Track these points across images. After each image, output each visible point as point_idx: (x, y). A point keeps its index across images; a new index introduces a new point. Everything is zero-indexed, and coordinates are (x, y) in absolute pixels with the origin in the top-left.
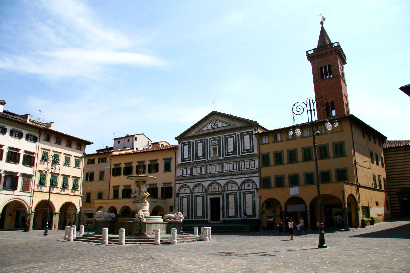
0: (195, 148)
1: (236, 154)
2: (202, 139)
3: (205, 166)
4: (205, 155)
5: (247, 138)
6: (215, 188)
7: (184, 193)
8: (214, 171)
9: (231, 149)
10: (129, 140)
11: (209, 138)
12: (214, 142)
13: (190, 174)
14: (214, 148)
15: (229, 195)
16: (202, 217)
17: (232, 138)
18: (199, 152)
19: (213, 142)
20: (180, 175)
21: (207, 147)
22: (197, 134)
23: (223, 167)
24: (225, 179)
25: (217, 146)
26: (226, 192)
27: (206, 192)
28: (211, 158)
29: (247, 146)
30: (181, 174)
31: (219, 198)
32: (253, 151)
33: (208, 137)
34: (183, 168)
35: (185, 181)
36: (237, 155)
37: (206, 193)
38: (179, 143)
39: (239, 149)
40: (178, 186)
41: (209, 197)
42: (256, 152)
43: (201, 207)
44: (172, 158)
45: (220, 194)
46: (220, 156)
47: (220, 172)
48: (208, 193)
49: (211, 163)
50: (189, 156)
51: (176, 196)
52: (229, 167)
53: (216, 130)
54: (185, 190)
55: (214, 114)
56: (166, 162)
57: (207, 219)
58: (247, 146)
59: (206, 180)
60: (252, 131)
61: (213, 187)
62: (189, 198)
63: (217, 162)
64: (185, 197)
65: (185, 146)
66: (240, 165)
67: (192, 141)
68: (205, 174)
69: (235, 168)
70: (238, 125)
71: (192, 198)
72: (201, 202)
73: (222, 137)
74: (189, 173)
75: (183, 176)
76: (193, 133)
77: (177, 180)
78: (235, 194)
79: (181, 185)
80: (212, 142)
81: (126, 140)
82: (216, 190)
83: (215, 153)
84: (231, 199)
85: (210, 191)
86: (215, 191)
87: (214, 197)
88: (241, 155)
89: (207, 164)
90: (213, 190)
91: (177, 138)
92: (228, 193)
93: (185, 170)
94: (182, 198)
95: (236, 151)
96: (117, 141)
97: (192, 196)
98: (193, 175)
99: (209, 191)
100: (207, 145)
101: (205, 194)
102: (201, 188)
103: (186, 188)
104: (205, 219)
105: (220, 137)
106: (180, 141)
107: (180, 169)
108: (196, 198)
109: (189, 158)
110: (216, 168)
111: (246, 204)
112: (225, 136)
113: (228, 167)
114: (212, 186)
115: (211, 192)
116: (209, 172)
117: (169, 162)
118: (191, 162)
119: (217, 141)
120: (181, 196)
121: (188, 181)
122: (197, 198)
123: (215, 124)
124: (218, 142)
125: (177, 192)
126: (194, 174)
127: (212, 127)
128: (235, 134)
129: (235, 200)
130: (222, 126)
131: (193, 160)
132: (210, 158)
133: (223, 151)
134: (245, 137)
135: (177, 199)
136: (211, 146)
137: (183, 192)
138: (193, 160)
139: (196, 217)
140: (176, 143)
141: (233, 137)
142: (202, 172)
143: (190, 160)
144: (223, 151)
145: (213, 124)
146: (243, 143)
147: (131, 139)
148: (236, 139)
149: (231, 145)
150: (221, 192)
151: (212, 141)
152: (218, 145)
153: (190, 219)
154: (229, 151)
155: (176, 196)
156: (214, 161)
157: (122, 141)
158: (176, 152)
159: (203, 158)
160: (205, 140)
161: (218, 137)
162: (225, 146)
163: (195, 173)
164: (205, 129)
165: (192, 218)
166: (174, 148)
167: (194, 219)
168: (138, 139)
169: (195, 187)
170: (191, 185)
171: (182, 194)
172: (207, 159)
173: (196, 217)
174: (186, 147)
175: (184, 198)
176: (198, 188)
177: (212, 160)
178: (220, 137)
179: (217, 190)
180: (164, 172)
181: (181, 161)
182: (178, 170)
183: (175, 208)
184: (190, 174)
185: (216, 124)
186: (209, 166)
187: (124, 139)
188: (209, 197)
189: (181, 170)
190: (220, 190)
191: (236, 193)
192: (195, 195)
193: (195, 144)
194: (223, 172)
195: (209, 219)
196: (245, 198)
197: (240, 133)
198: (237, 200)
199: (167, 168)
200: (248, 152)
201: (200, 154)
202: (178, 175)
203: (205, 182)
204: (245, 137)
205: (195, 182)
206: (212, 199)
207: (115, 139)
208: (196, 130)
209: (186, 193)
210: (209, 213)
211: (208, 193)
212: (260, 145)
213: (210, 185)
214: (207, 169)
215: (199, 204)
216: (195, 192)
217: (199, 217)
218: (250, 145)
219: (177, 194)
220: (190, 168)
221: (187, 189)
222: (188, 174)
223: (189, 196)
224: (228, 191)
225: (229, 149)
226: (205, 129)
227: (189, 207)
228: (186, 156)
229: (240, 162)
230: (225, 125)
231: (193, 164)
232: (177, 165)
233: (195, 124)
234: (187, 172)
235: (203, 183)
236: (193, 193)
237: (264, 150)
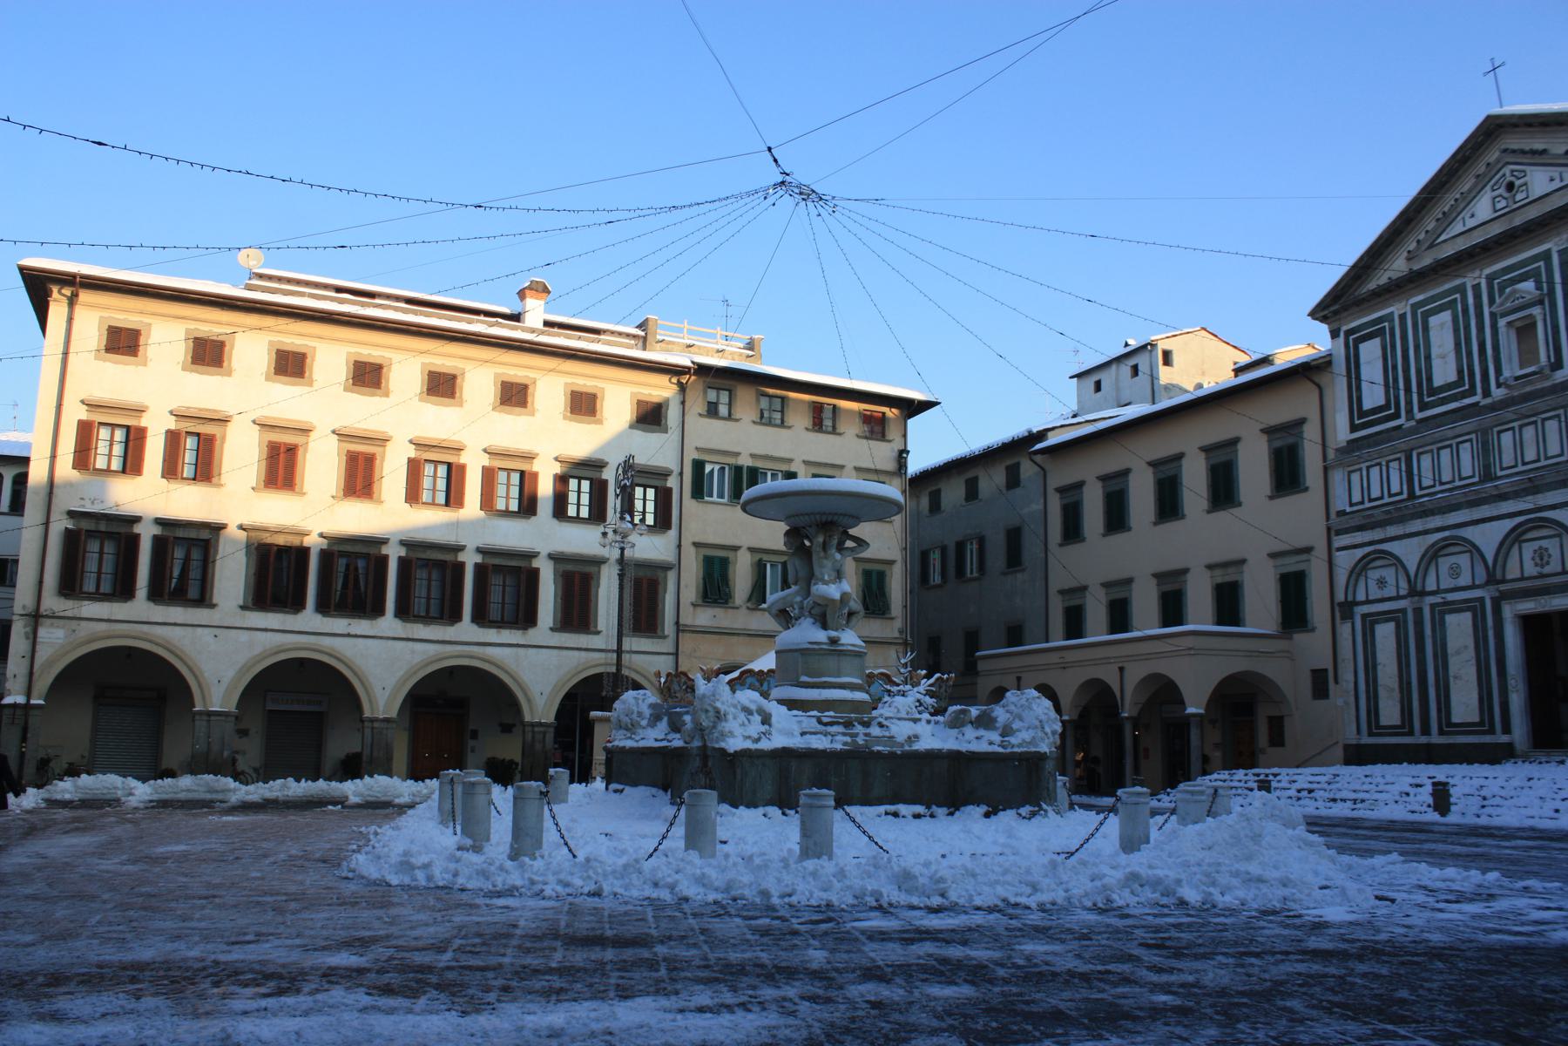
0: (1417, 348)
2: (1447, 286)
3: (1473, 436)
6: (1541, 556)
8: (1530, 455)
10: (1135, 370)
11: (1487, 271)
12: (1514, 291)
13: (1401, 493)
14: (1519, 324)
16: (1481, 723)
18: (1436, 363)
20: (1351, 505)
21: (1481, 329)
22: (1417, 266)
25: (1536, 311)
27: (1492, 580)
28: (1508, 387)
30: (1356, 497)
33: (1477, 273)
34: (1364, 466)
35: (1377, 534)
37: (1491, 588)
38: (1334, 334)
40: (1345, 561)
43: (1473, 670)
44: (1301, 422)
48: (1503, 587)
49: (1507, 414)
51: (1338, 614)
53: (1518, 220)
56: (1278, 444)
57: (1504, 739)
59: (1488, 514)
61: (1529, 550)
62: (1405, 622)
63: (1536, 404)
64: (1386, 616)
65: (1362, 347)
67: (1396, 309)
68: (1476, 479)
72: (1471, 643)
74: (1395, 488)
75: (1368, 505)
76: (1398, 266)
77: (1338, 533)
81: (1125, 369)
82: (1547, 570)
83: (1527, 352)
85: (1513, 572)
86: (1542, 576)
87: (1540, 609)
90: (1530, 569)
93: (1375, 472)
94: (1371, 622)
96: (1090, 382)
98: (1418, 493)
99: (1509, 576)
100: (1480, 315)
102: (1464, 560)
106: (1335, 326)
107: (1350, 473)
108: (1443, 623)
109: (1389, 409)
110: (1541, 439)
114: (1524, 545)
115: (1522, 579)
116: (1502, 469)
117: (1291, 440)
118: (1399, 427)
119: (1528, 286)
120: (1364, 616)
121: (1392, 531)
123: (1510, 187)
124: (1539, 288)
125: (1340, 597)
127: (1499, 206)
130: (1557, 184)
131: (1410, 411)
132: (1499, 386)
135: (1345, 630)
136: (1503, 315)
137: (1375, 593)
139: (1450, 724)
142: (1464, 474)
143: (1397, 416)
145: (1502, 191)
147: (1142, 361)
151: (1501, 291)
152: (1541, 302)
155: (1338, 614)
157: (1106, 378)
159: (1464, 395)
161: (1535, 258)
164: (1458, 228)
165: (1426, 731)
167: (1436, 739)
168: (1176, 358)
169: (1432, 555)
170: (1410, 552)
171: (1368, 602)
172: (1487, 393)
173: (1447, 726)
174: (1370, 351)
175: (1378, 622)
176: (1445, 563)
177: (1513, 398)
178: (1546, 256)
180: (1271, 498)
181: (1354, 428)
182: (1338, 477)
183: (1336, 682)
185: (1517, 183)
186: (1499, 433)
187: (1114, 367)
189: (1355, 477)
192: (1433, 606)
199: (1286, 475)
201: (1444, 372)
202: (1340, 502)
203: (1481, 526)
205: (1426, 532)
206: (1532, 625)
207: (1079, 376)
210: (1517, 701)
211: (1503, 587)
213: (1514, 538)
214: (1486, 451)
215: (1458, 653)
216: (1434, 588)
217: (1466, 728)
219: (1340, 604)
221: (1389, 574)
222: (1390, 495)
223: (1403, 611)
226: (1458, 228)
231: (1412, 431)
232: (1331, 455)
233: (1403, 213)
234: (1382, 481)
235: (1468, 533)
236: (1424, 593)
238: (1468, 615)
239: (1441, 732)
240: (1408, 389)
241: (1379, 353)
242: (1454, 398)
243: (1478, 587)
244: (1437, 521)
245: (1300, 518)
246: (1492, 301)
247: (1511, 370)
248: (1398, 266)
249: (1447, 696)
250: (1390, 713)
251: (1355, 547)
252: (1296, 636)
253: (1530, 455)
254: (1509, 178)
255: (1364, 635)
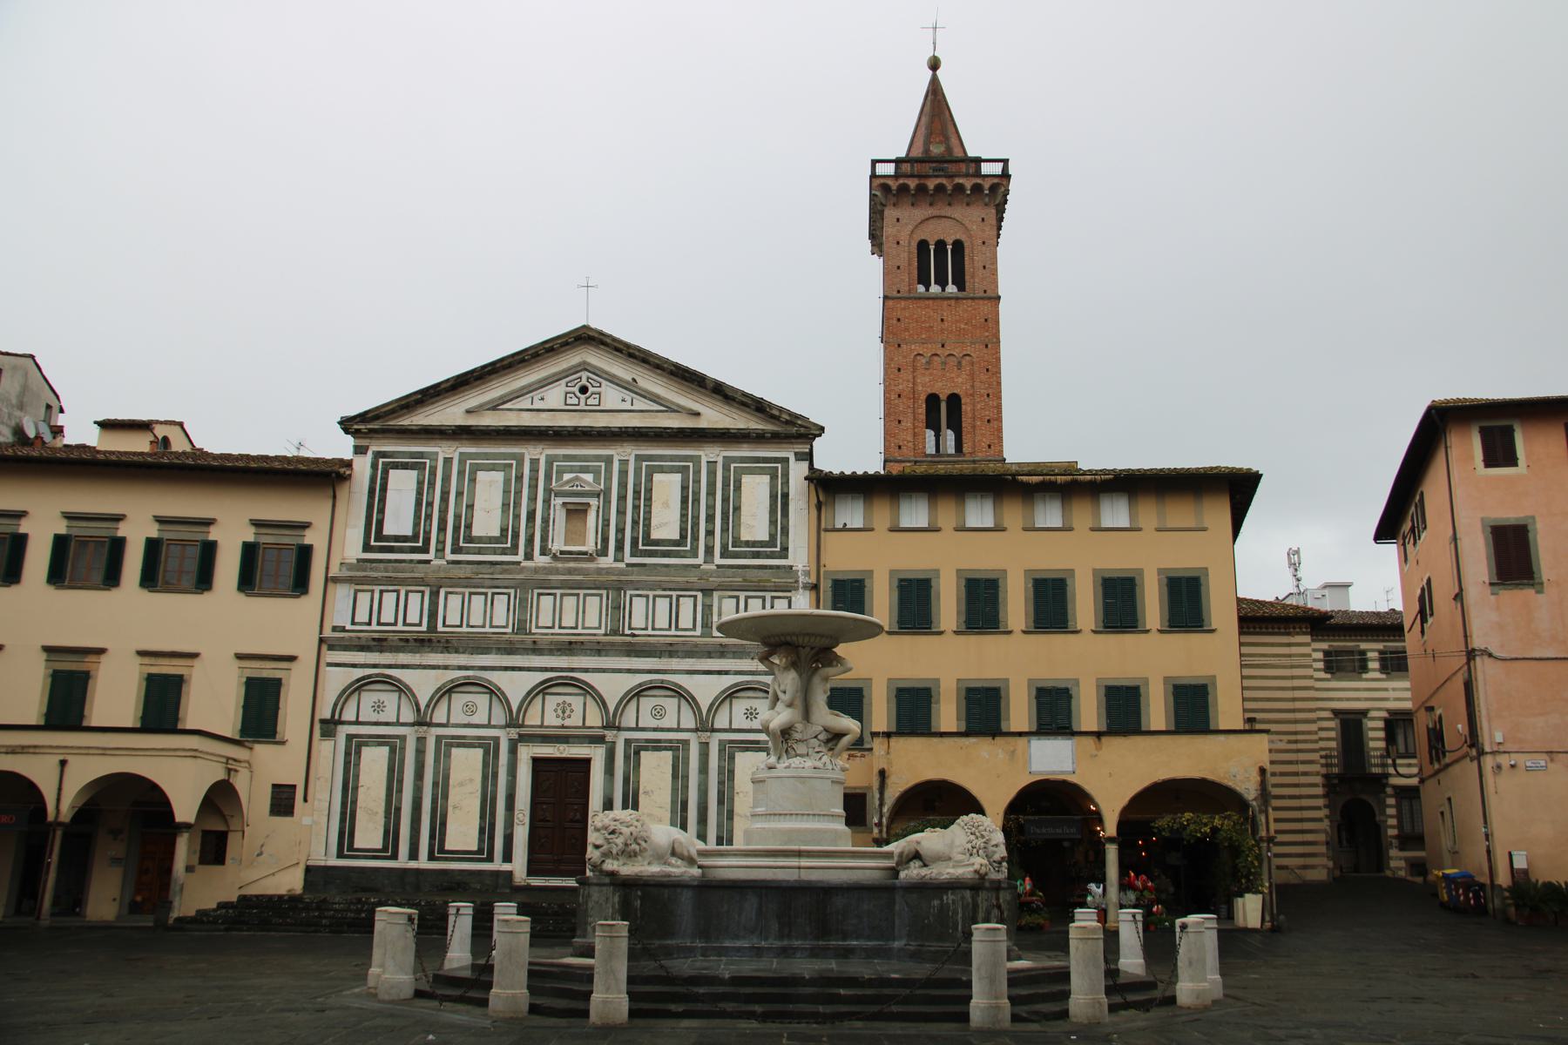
0: (459, 494)
1: (694, 553)
4: (516, 535)
5: (756, 490)
6: (564, 710)
7: (374, 717)
8: (569, 620)
9: (666, 524)
12: (577, 478)
15: (646, 749)
17: (678, 477)
19: (567, 477)
20: (353, 623)
23: (617, 609)
24: (629, 671)
25: (593, 502)
26: (620, 739)
27: (512, 722)
28: (555, 557)
29: (755, 525)
30: (362, 616)
31: (586, 763)
32: (784, 552)
33: (539, 450)
36: (700, 560)
38: (360, 450)
39: (710, 533)
40: (336, 681)
41: (526, 753)
42: (799, 557)
45: (599, 740)
46: (603, 552)
47: (602, 631)
48: (523, 731)
50: (416, 524)
51: (317, 727)
52: (651, 614)
54: (379, 707)
55: (584, 337)
57: (506, 867)
58: (755, 525)
60: (787, 460)
61: (552, 702)
62: (403, 749)
64: (380, 740)
66: (715, 609)
67: (443, 450)
69: (686, 620)
70: (714, 416)
71: (420, 752)
73: (624, 463)
74: (413, 617)
76: (451, 413)
77: (331, 648)
78: (674, 749)
79: (360, 673)
80: (559, 478)
82: (568, 722)
84: (655, 771)
86: (563, 727)
88: (718, 560)
89: (528, 586)
90: (552, 720)
91: (348, 425)
92: (637, 740)
94: (355, 747)
95: (695, 538)
97: (421, 741)
98: (440, 628)
100: (533, 487)
101: (504, 736)
103: (383, 696)
104: (497, 865)
105: (609, 460)
108: (448, 755)
109: (417, 541)
110: (581, 611)
111: (732, 800)
112: (639, 458)
113: (648, 614)
115: (542, 726)
118: (428, 562)
119: (589, 477)
120: (350, 737)
121: (403, 658)
122: (454, 750)
123: (584, 390)
124: (597, 480)
126: (444, 625)
128: (696, 460)
129: (675, 776)
131: (440, 551)
132: (543, 553)
133: (620, 530)
134: (746, 480)
137: (367, 714)
138: (440, 551)
140: (340, 446)
141: (683, 471)
143: (425, 549)
144: (620, 530)
145: (576, 389)
146: (732, 510)
148: (697, 481)
149: (666, 505)
150: (600, 732)
151: (560, 472)
152: (598, 496)
153: (403, 862)
154: (655, 535)
156: (573, 578)
158: (335, 497)
159: (504, 552)
160: (520, 459)
161: (598, 458)
162: (636, 508)
163: (453, 618)
164: (525, 403)
165: (414, 855)
166: (322, 477)
167: (423, 863)
170: (424, 684)
171: (357, 723)
172: (529, 556)
174: (402, 485)
179: (575, 720)
181: (367, 547)
183: (305, 800)
184: (420, 624)
185: (591, 390)
188: (526, 753)
189: (364, 599)
190: (595, 719)
191: (686, 743)
192: (439, 739)
193: (461, 473)
194: (615, 632)
195: (518, 867)
196: (732, 772)
197: (720, 460)
198: (686, 777)
200: (757, 555)
201: (487, 522)
204: (746, 480)
205: (446, 667)
208: (474, 398)
209: (387, 724)
212: (826, 530)
213: (543, 689)
215: (461, 784)
218: (773, 522)
219: (323, 721)
220: (423, 592)
222: (405, 624)
224: (637, 729)
225: (654, 522)
227: (400, 800)
228: (399, 521)
229: (716, 595)
230: (641, 404)
235: (496, 678)
236: (430, 725)
237: (844, 557)
238: (479, 752)
239: (431, 857)
240: (442, 528)
241: (414, 486)
242: (494, 552)
243: (494, 727)
244: (462, 659)
245: (283, 624)
246: (548, 477)
247: (557, 545)
248: (451, 413)
249: (444, 824)
250: (369, 835)
251: (354, 666)
252: (258, 747)
253: (569, 620)
254: (584, 382)
255: (348, 754)
